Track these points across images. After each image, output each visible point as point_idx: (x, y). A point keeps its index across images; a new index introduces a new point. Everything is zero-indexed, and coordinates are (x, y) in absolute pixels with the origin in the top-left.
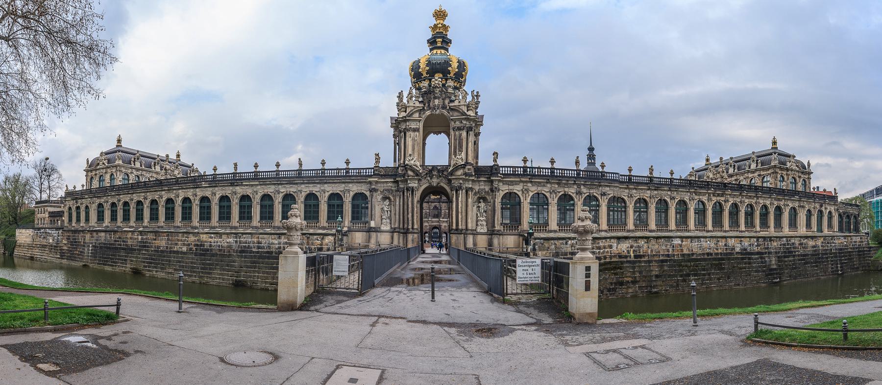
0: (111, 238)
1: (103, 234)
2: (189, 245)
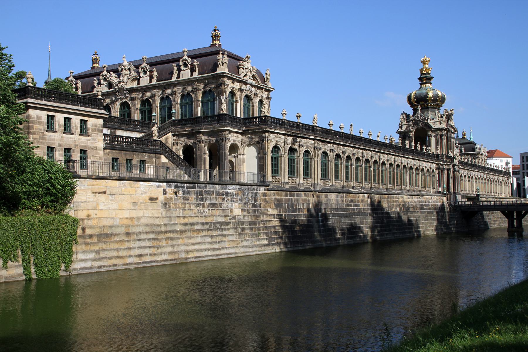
0: (343, 201)
1: (333, 196)
2: (399, 205)
